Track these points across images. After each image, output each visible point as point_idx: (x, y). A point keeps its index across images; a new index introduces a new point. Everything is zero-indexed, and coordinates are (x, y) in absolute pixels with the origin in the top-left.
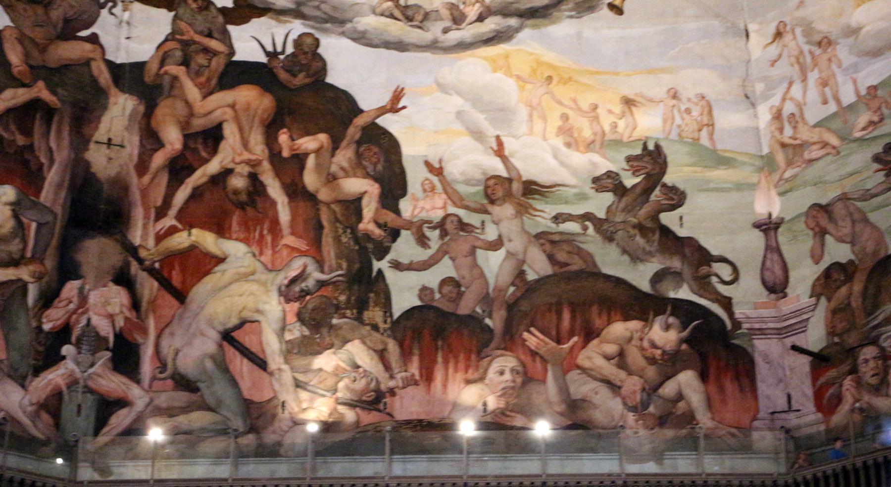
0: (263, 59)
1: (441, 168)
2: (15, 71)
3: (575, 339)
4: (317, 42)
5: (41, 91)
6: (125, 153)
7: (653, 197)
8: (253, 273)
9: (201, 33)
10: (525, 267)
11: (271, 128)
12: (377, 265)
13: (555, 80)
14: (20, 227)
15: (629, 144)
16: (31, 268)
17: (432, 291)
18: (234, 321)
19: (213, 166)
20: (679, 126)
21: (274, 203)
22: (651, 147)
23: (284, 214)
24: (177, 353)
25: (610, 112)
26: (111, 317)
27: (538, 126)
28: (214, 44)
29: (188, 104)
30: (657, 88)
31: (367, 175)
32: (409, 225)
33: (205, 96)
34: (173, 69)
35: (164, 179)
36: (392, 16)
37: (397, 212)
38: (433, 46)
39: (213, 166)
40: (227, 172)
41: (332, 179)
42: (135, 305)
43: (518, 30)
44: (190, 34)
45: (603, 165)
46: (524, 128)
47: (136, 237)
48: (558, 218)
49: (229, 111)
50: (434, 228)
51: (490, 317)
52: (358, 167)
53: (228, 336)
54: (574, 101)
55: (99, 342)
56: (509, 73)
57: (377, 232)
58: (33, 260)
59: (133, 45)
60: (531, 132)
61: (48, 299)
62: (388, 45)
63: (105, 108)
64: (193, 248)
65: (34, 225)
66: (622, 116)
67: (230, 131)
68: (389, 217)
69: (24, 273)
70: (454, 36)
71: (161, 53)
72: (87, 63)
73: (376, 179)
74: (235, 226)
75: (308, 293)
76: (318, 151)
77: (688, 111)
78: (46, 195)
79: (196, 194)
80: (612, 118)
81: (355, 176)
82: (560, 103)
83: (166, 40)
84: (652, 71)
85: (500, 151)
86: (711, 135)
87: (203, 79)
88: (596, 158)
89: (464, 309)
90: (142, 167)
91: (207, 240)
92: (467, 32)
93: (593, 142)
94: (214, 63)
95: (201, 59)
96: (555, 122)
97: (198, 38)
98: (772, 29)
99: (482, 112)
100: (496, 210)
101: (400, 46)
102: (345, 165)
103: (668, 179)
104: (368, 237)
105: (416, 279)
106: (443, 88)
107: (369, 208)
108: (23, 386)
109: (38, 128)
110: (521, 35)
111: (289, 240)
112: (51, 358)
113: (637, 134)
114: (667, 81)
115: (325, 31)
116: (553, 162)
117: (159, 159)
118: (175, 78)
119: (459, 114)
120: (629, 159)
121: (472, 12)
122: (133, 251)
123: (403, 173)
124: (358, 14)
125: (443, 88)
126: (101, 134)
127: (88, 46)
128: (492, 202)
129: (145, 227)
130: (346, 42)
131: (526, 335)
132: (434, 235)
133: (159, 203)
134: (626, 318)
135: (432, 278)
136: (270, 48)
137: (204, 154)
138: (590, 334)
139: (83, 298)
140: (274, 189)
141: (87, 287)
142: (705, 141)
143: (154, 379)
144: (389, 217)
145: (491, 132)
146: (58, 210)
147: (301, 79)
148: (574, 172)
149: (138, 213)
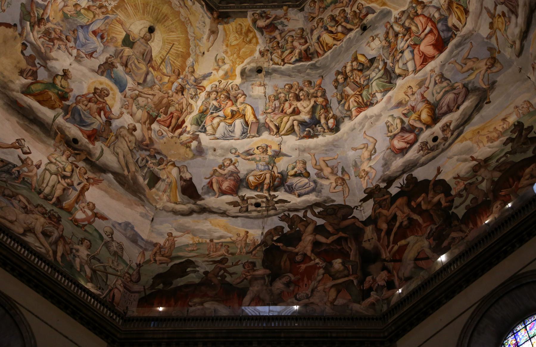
0: (399, 190)
1: (459, 176)
2: (331, 232)
3: (516, 183)
4: (412, 175)
5: (341, 234)
6: (374, 240)
7: (523, 134)
8: (418, 240)
9: (382, 197)
10: (493, 179)
11: (409, 204)
12: (450, 212)
13: (480, 131)
14: (346, 268)
15: (510, 128)
16: (353, 276)
17: (469, 205)
18: (416, 254)
19: (398, 224)
20: (522, 113)
21: (417, 220)
22: (516, 123)
23: (420, 221)
24: (404, 274)
25: (500, 125)
26: (384, 280)
27: (481, 145)
28: (386, 197)
29: (385, 215)
30: (511, 109)
31: (439, 194)
32: (456, 196)
33: (388, 211)
34: (378, 211)
35: (386, 237)
36: (428, 153)
37: (451, 195)
38: (443, 150)
39: (398, 224)
40: (401, 223)
41: (430, 202)
42: (389, 272)
43: (464, 129)
44: (378, 199)
45: (504, 139)
46: (477, 148)
47: (384, 256)
48: (497, 161)
49: (396, 209)
50: (463, 190)
51: (488, 197)
52: (436, 193)
53: (416, 259)
54: (488, 131)
55: (383, 287)
56: (466, 140)
57: (448, 204)
58: (353, 274)
59: (366, 214)
60: (480, 148)
61: (361, 282)
62: (430, 160)
63: (364, 232)
64: (400, 247)
65: (350, 266)
66: (504, 123)
67: (399, 213)
68: (450, 198)
69: (351, 278)
70: (447, 144)
71: (374, 209)
72: (354, 224)
73: (442, 193)
74: (408, 233)
75: (434, 232)
76: (423, 199)
77: (523, 107)
78: (352, 258)
79: (396, 234)
80: (501, 127)
81: (436, 196)
82: (485, 135)
83: (374, 205)
84: (506, 108)
85: (473, 159)
86: (533, 107)
87: (386, 207)
88: (501, 139)
89: (480, 202)
90: (379, 239)
91: (403, 242)
92: (450, 141)
93: (499, 136)
94: (388, 201)
95: (384, 203)
96: (485, 140)
97: (381, 199)
98: (531, 69)
99: (464, 154)
100: (479, 173)
101: (434, 158)
102: (432, 196)
103: (525, 127)
104: (445, 207)
105: (463, 206)
106: (450, 158)
107: (443, 202)
108: (360, 304)
109: (343, 243)
110: (465, 129)
111: (424, 225)
112: (369, 296)
113: (510, 125)
114: (513, 106)
115: (413, 171)
116: (489, 149)
117: (383, 234)
118: (380, 212)
119: (458, 160)
120: (511, 132)
121: (449, 135)
122: (385, 260)
123: (449, 185)
124: (419, 160)
125: (450, 158)
126: (365, 238)
127: (353, 220)
128: (476, 172)
129: (385, 253)
130: (419, 169)
131: (500, 193)
132: (464, 193)
133: (387, 244)
134: (529, 166)
135: (468, 202)
136: (400, 186)
137: (394, 224)
138: (519, 179)
139: (374, 280)
140: (415, 217)
141: (375, 277)
142: (531, 109)
143: (399, 284)
144: (450, 198)
145: (468, 157)
146: (358, 261)
147: (411, 186)
148: (497, 147)
149: (382, 251)
